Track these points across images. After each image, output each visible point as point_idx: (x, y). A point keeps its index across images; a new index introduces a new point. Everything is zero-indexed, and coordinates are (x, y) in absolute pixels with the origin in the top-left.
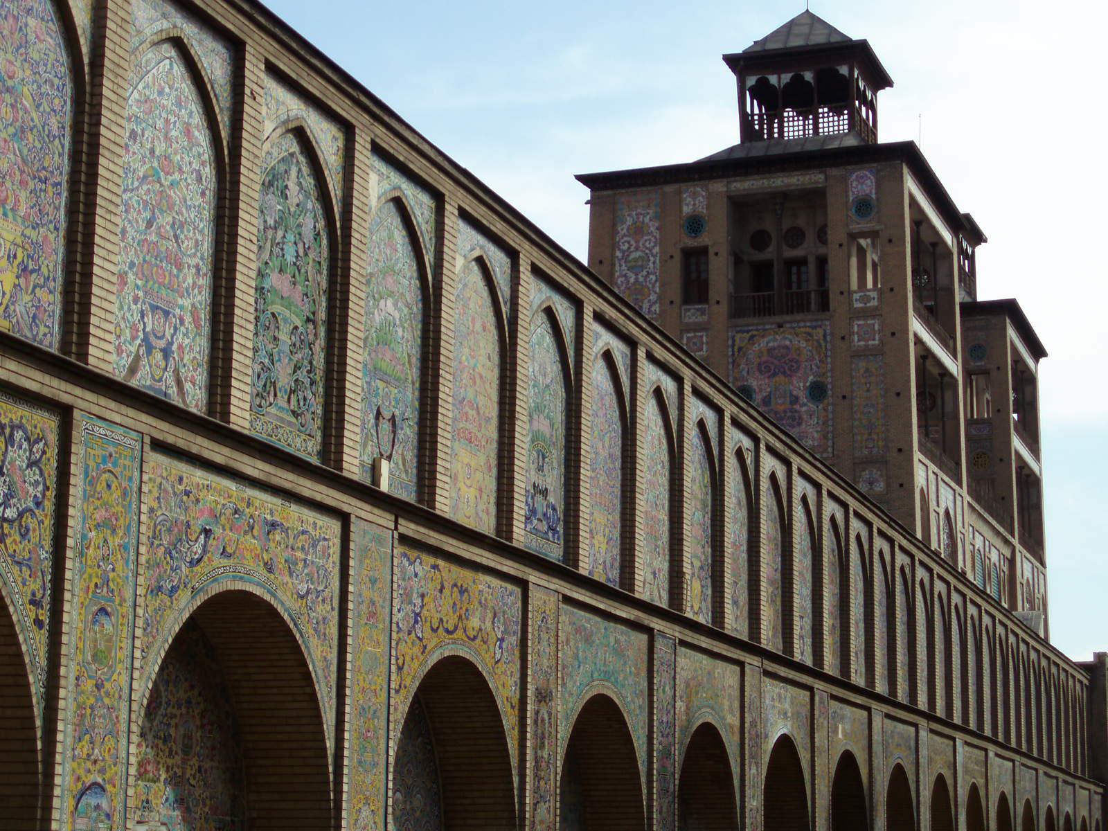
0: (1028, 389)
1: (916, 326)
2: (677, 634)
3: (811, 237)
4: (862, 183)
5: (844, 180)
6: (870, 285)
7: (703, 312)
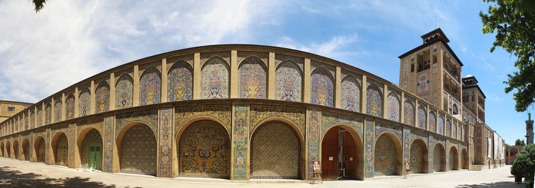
7: (413, 73)
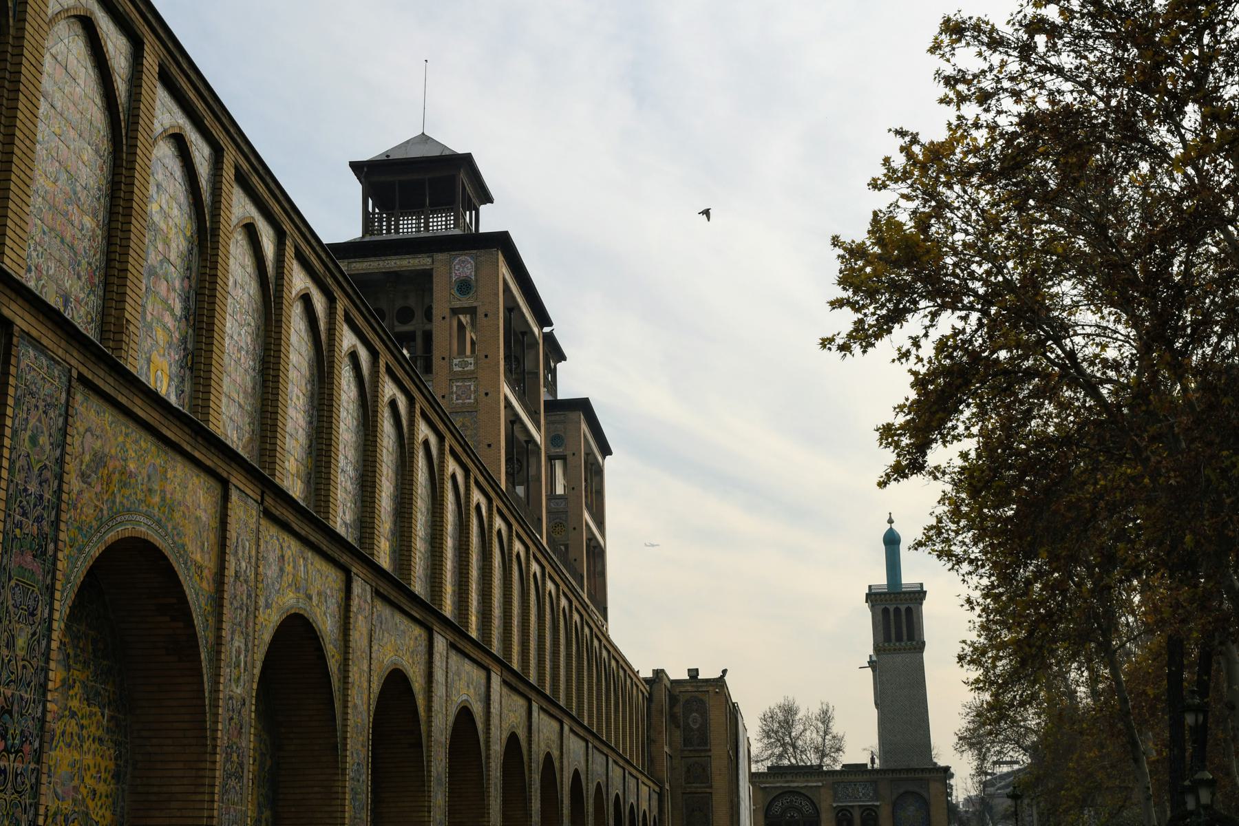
0: (595, 479)
1: (506, 390)
2: (73, 362)
3: (419, 314)
4: (464, 266)
5: (450, 262)
6: (468, 352)
